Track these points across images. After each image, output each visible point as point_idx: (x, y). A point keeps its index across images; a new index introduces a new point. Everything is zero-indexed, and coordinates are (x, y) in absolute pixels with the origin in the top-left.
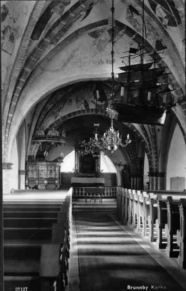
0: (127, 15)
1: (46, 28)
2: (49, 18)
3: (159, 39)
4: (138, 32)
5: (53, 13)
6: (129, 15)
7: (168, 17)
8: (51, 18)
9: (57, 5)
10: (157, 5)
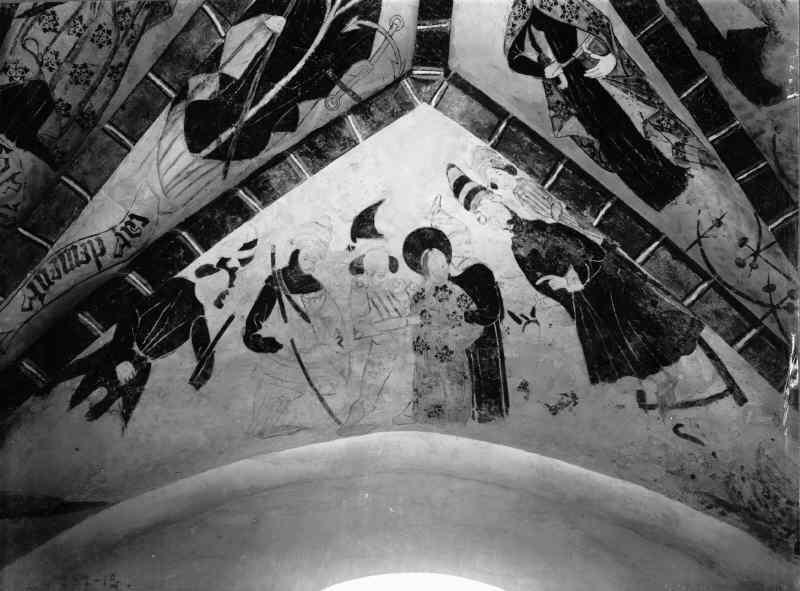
3: (57, 94)
7: (234, 92)
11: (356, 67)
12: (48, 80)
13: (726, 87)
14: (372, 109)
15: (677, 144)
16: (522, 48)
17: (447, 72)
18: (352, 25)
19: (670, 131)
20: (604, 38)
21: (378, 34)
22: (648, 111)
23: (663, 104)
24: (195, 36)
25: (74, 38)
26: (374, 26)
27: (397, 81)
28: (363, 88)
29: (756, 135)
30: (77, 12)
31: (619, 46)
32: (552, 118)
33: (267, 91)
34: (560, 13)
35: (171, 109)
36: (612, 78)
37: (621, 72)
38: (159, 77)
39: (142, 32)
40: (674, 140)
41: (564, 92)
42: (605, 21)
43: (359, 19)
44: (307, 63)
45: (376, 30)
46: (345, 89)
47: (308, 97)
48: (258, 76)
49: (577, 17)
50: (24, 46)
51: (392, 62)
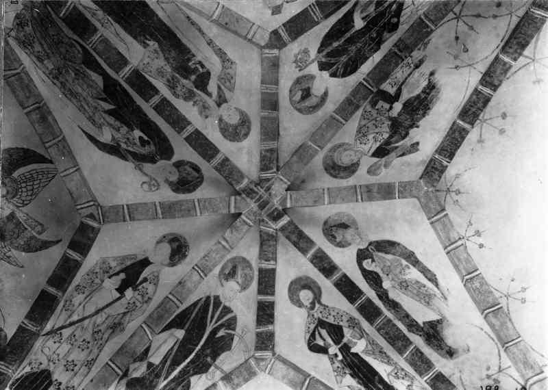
0: (115, 259)
1: (100, 13)
2: (130, 33)
3: (55, 377)
4: (61, 304)
5: (145, 46)
6: (113, 264)
8: (129, 39)
9: (167, 59)
10: (182, 328)
11: (223, 356)
12: (51, 369)
13: (428, 351)
14: (233, 377)
15: (409, 386)
16: (315, 339)
17: (274, 354)
18: (221, 333)
19: (403, 378)
20: (358, 330)
21: (235, 337)
22: (389, 368)
23: (396, 363)
24: (136, 339)
25: (70, 346)
26: (233, 332)
27: (246, 361)
28: (227, 368)
29: (450, 377)
30: (73, 332)
31: (367, 334)
32: (336, 376)
33: (173, 370)
34: (333, 319)
35: (118, 383)
36: (366, 352)
37: (370, 347)
38: (114, 363)
39: (106, 342)
40: (407, 383)
41: (342, 361)
42: (356, 321)
43: (226, 329)
44: (196, 354)
45: (234, 335)
46: (217, 368)
47: (196, 373)
48: (168, 363)
49: (342, 321)
50: (42, 351)
51: (244, 351)
